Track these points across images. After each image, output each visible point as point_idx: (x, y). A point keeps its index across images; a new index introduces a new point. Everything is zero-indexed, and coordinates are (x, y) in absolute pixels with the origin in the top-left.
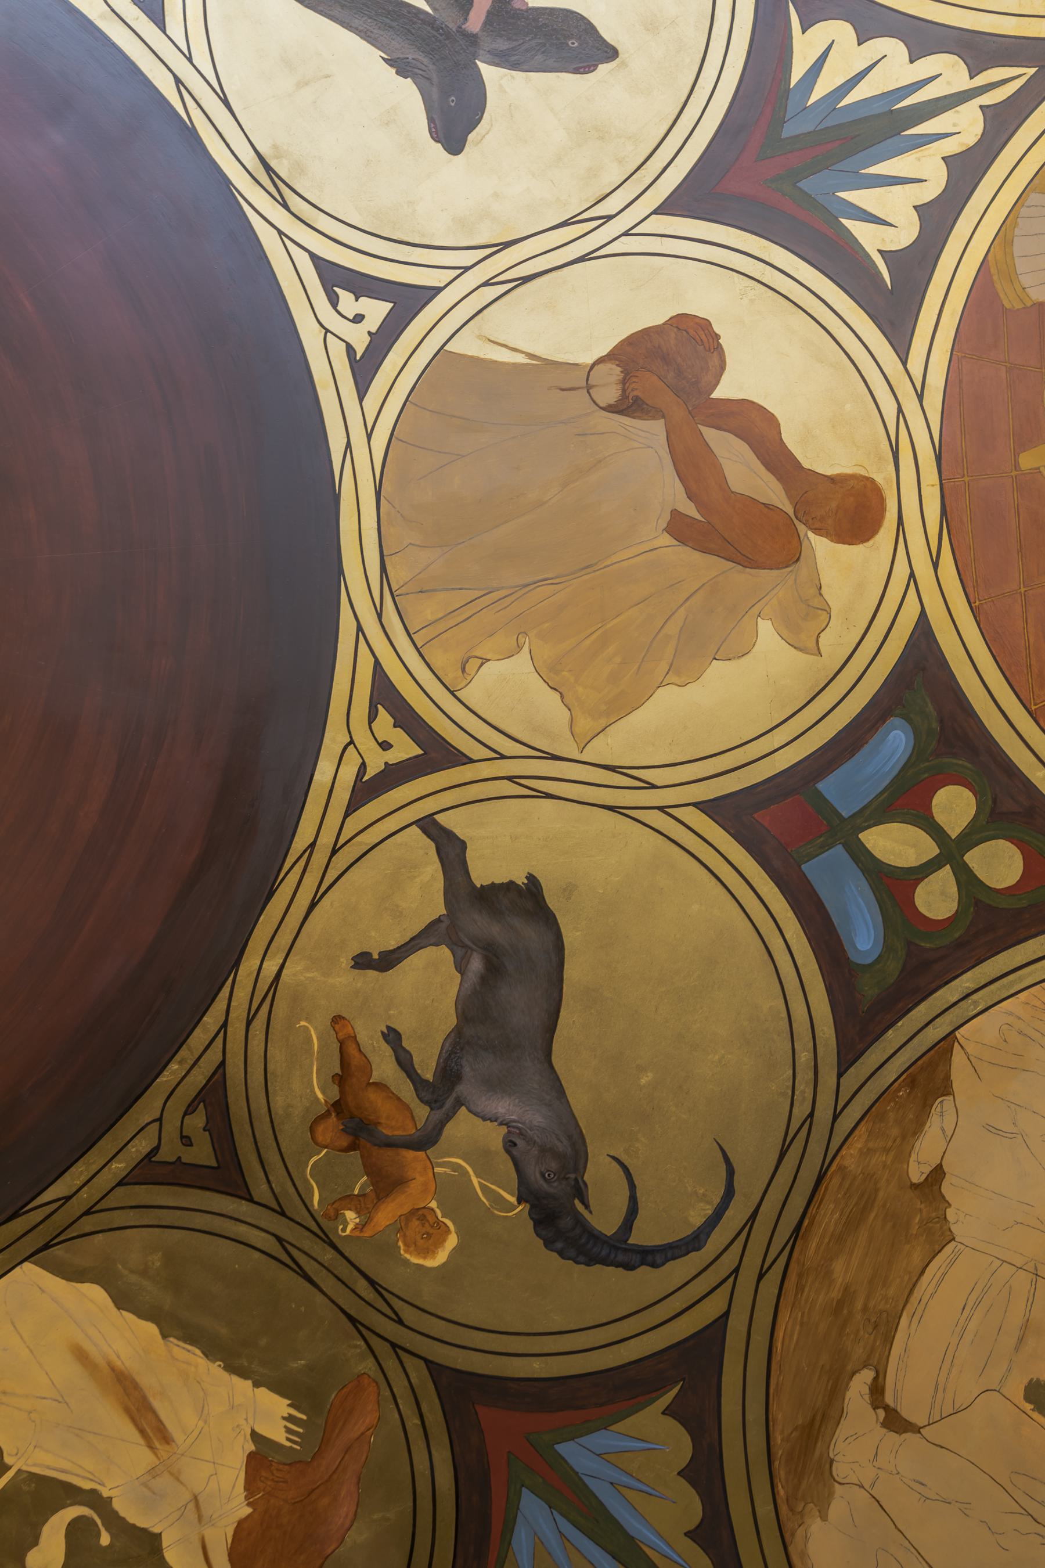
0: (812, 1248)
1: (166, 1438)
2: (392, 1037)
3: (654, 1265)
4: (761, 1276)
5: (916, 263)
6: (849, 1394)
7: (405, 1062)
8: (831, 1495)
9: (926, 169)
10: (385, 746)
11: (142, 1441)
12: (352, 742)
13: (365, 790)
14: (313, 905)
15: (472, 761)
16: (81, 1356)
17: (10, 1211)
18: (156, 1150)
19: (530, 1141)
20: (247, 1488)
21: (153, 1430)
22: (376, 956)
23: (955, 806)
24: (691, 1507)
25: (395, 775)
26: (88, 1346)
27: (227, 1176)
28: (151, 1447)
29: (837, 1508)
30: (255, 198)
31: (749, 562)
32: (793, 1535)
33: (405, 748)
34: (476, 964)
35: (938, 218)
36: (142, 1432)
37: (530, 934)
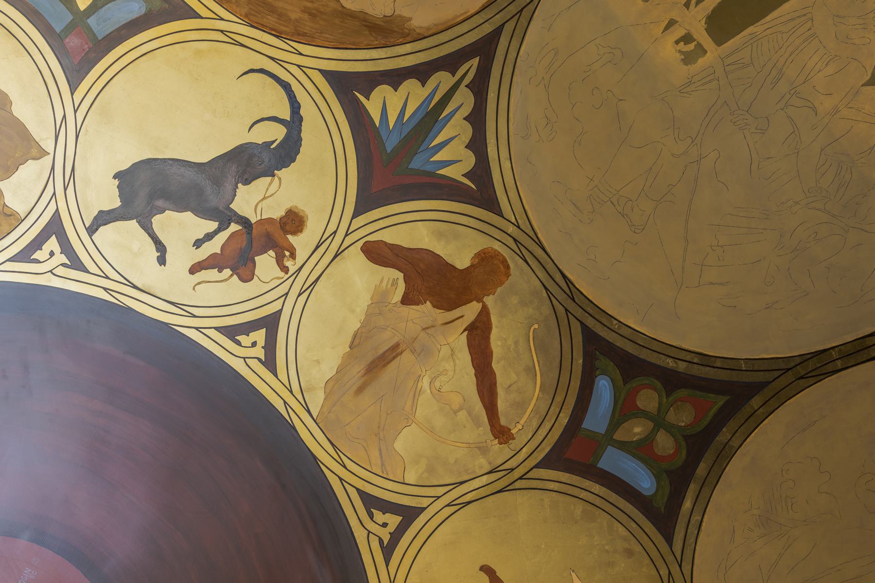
1: (397, 345)
2: (198, 244)
3: (299, 107)
4: (301, 54)
6: (353, 9)
7: (209, 237)
8: (400, 16)
10: (52, 254)
11: (399, 358)
12: (51, 271)
13: (76, 264)
14: (135, 287)
15: (57, 209)
16: (360, 390)
17: (293, 431)
18: (259, 360)
19: (244, 172)
20: (417, 303)
21: (394, 352)
22: (159, 254)
24: (410, 85)
25: (66, 248)
26: (355, 388)
27: (270, 323)
28: (401, 353)
29: (405, 13)
32: (420, 34)
33: (52, 244)
34: (160, 203)
36: (394, 358)
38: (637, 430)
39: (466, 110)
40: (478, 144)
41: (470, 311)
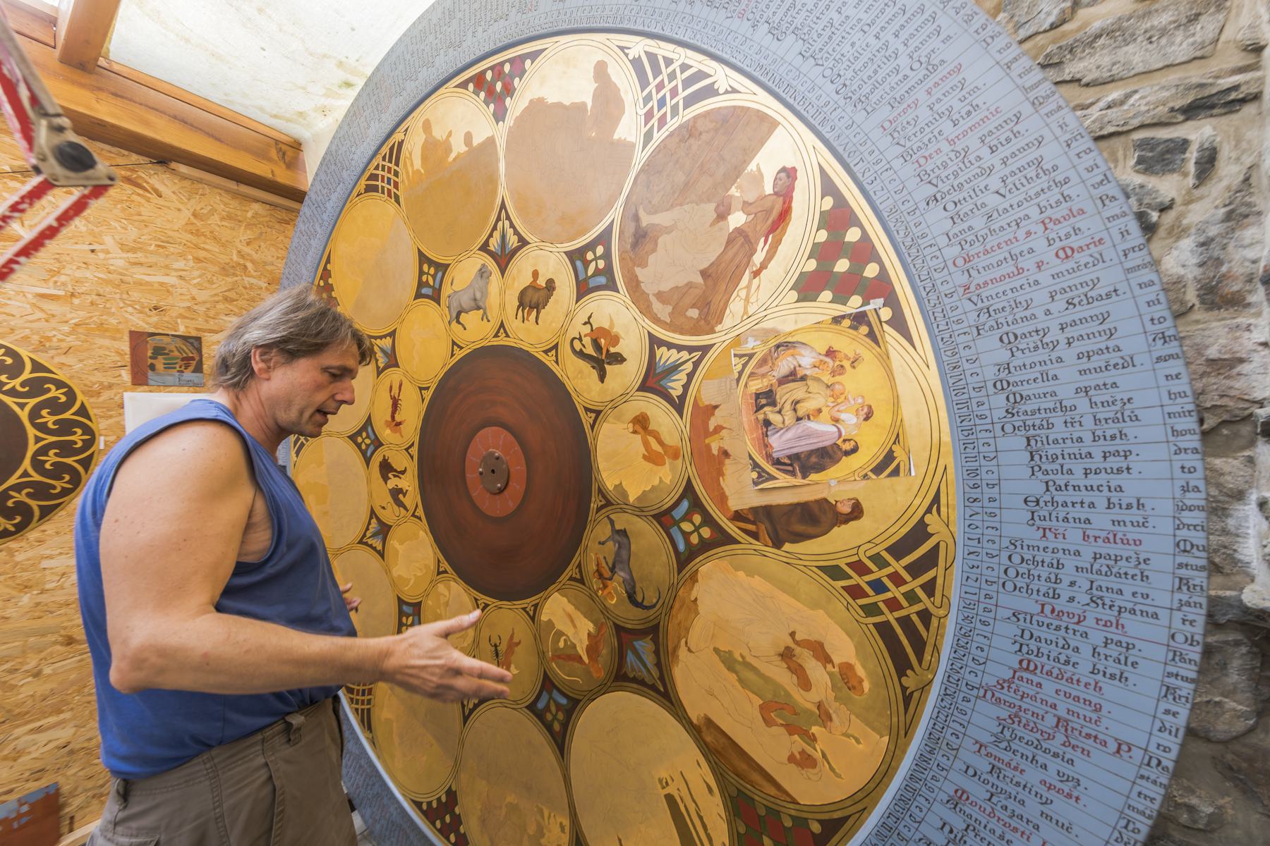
0: (674, 612)
5: (682, 398)
9: (682, 377)
21: (575, 626)
23: (697, 519)
27: (582, 581)
30: (574, 395)
31: (657, 464)
35: (686, 387)
37: (625, 540)
38: (553, 708)
39: (647, 680)
40: (634, 680)
41: (585, 659)
